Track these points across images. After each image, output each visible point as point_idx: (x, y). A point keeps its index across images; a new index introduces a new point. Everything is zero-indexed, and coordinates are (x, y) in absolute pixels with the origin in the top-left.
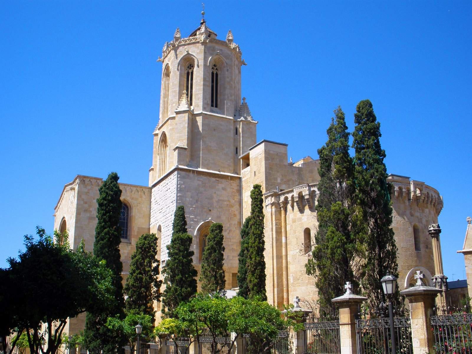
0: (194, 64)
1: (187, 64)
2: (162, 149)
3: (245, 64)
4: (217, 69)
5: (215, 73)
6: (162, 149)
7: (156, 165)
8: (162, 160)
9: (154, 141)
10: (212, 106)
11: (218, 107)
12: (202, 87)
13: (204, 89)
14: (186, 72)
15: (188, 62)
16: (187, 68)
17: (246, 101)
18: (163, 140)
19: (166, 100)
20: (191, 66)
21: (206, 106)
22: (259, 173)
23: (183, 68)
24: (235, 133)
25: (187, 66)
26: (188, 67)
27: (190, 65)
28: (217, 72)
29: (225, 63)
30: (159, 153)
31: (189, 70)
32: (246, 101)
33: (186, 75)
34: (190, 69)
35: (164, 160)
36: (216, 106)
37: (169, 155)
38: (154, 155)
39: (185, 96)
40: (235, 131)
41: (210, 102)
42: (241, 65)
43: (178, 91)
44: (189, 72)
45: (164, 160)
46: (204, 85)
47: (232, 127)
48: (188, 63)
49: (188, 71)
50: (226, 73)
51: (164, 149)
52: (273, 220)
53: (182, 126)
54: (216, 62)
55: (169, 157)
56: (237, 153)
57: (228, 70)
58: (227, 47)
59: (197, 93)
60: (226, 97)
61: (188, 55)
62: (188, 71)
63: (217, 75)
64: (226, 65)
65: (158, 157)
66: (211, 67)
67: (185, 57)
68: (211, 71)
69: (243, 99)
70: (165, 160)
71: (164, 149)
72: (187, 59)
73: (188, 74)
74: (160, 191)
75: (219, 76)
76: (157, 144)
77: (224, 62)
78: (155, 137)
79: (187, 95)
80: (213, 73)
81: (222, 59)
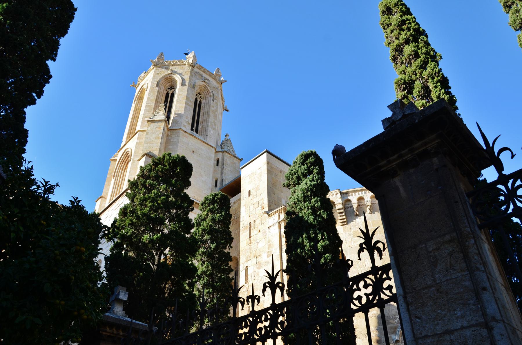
0: (176, 87)
1: (168, 85)
2: (120, 171)
3: (227, 111)
4: (201, 97)
5: (199, 100)
6: (120, 171)
7: (107, 194)
8: (117, 184)
9: (110, 167)
10: (192, 130)
11: (199, 132)
12: (184, 105)
13: (185, 107)
14: (165, 92)
15: (169, 83)
16: (167, 89)
17: (228, 138)
18: (124, 161)
19: (135, 121)
20: (173, 88)
21: (186, 124)
22: (257, 189)
23: (163, 87)
24: (216, 165)
25: (168, 88)
26: (169, 89)
27: (171, 87)
28: (200, 100)
29: (211, 93)
30: (115, 176)
31: (169, 91)
32: (228, 138)
33: (165, 95)
34: (171, 90)
35: (120, 183)
36: (197, 132)
37: (130, 171)
38: (108, 176)
39: (163, 108)
40: (216, 162)
41: (191, 122)
42: (223, 111)
43: (153, 106)
44: (169, 93)
45: (120, 183)
46: (186, 104)
47: (213, 156)
48: (169, 84)
49: (168, 92)
50: (212, 102)
51: (123, 172)
52: (283, 244)
53: (154, 136)
54: (201, 90)
55: (130, 172)
56: (216, 185)
57: (213, 100)
58: (214, 79)
59: (177, 110)
60: (210, 124)
61: (170, 75)
62: (168, 92)
63: (200, 102)
64: (212, 95)
65: (113, 180)
66: (195, 94)
67: (166, 77)
68: (195, 97)
69: (226, 136)
70: (122, 184)
71: (123, 172)
72: (169, 80)
73: (167, 94)
74: (109, 217)
75: (202, 105)
76: (114, 167)
77: (211, 91)
78: (112, 162)
79: (165, 109)
80: (196, 100)
81: (208, 88)
